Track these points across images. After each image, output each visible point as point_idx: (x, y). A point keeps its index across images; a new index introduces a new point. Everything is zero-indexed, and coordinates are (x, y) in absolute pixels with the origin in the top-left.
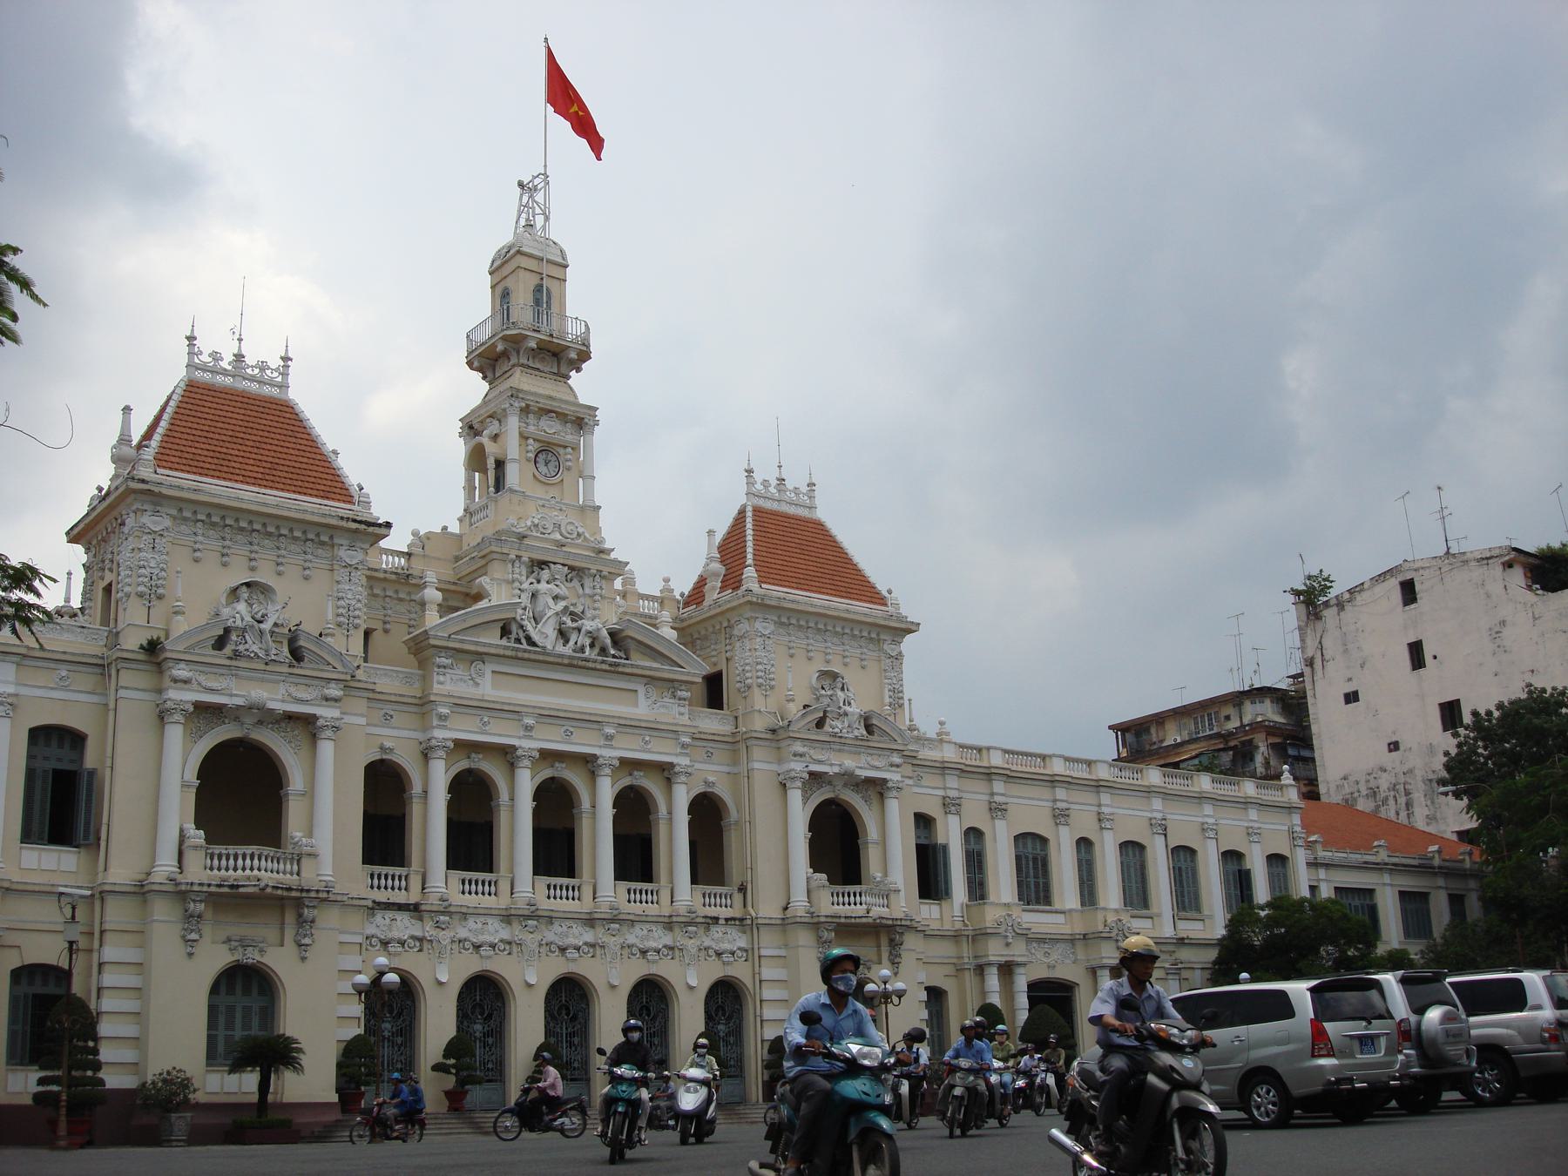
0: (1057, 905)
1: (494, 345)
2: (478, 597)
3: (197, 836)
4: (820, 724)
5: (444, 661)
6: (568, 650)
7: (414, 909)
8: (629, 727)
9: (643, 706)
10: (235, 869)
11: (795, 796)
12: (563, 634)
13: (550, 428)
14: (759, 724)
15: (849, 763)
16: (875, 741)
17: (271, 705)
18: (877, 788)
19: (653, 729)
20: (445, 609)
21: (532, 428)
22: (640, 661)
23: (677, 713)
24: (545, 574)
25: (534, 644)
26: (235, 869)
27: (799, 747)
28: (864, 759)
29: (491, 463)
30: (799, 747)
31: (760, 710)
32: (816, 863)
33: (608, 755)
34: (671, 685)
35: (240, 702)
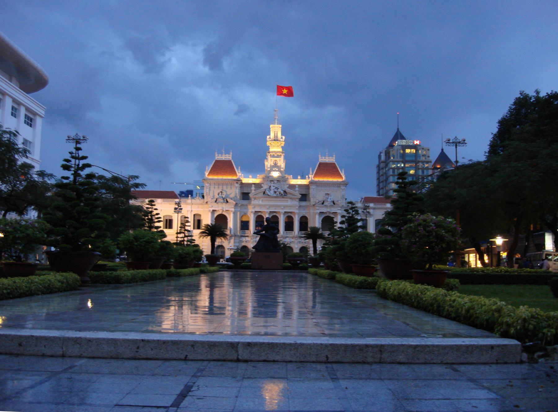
4: (323, 203)
6: (275, 195)
7: (248, 236)
8: (285, 207)
9: (289, 203)
11: (317, 216)
12: (275, 192)
14: (312, 203)
15: (328, 210)
16: (334, 206)
19: (290, 206)
20: (255, 190)
22: (289, 196)
23: (296, 203)
27: (317, 208)
28: (333, 209)
30: (317, 208)
31: (312, 201)
34: (295, 199)
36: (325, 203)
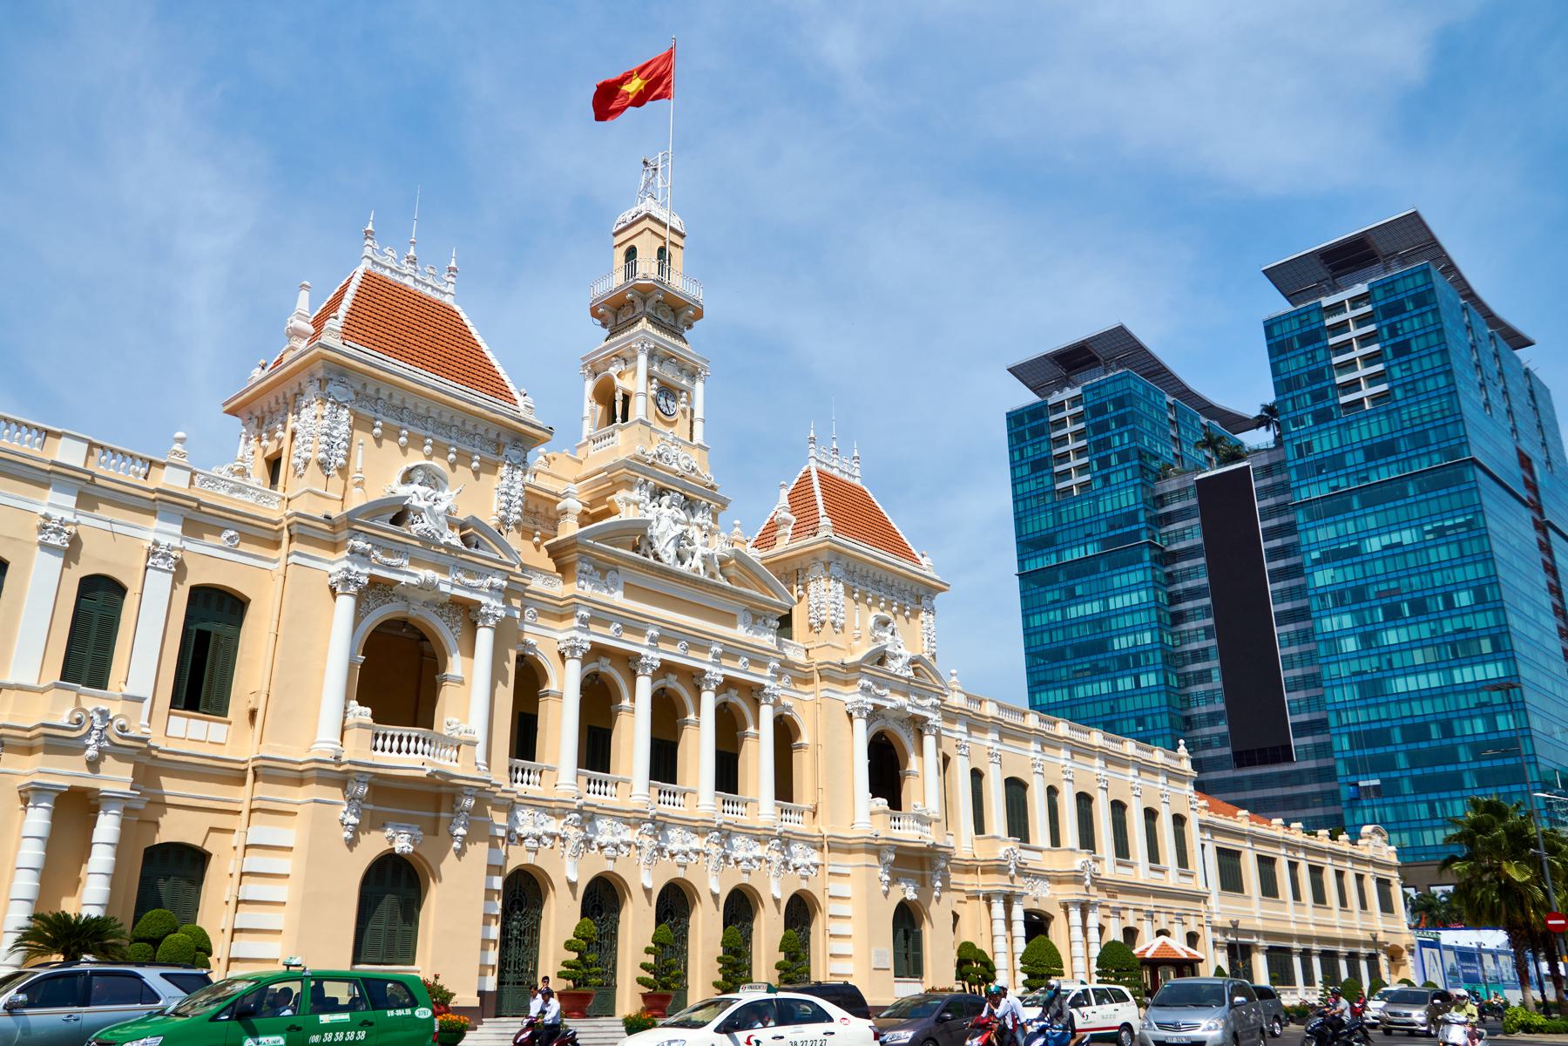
0: (1032, 843)
1: (624, 294)
2: (608, 513)
3: (364, 714)
5: (586, 567)
10: (408, 751)
13: (669, 374)
17: (444, 588)
18: (918, 725)
21: (656, 368)
24: (666, 500)
25: (659, 559)
26: (408, 751)
29: (619, 396)
32: (876, 789)
33: (716, 673)
35: (413, 581)
36: (895, 666)
